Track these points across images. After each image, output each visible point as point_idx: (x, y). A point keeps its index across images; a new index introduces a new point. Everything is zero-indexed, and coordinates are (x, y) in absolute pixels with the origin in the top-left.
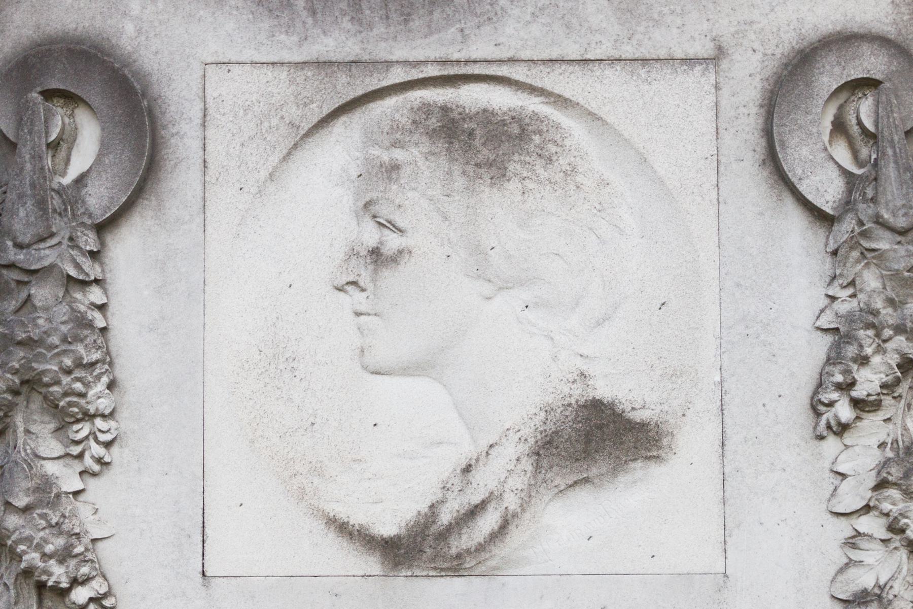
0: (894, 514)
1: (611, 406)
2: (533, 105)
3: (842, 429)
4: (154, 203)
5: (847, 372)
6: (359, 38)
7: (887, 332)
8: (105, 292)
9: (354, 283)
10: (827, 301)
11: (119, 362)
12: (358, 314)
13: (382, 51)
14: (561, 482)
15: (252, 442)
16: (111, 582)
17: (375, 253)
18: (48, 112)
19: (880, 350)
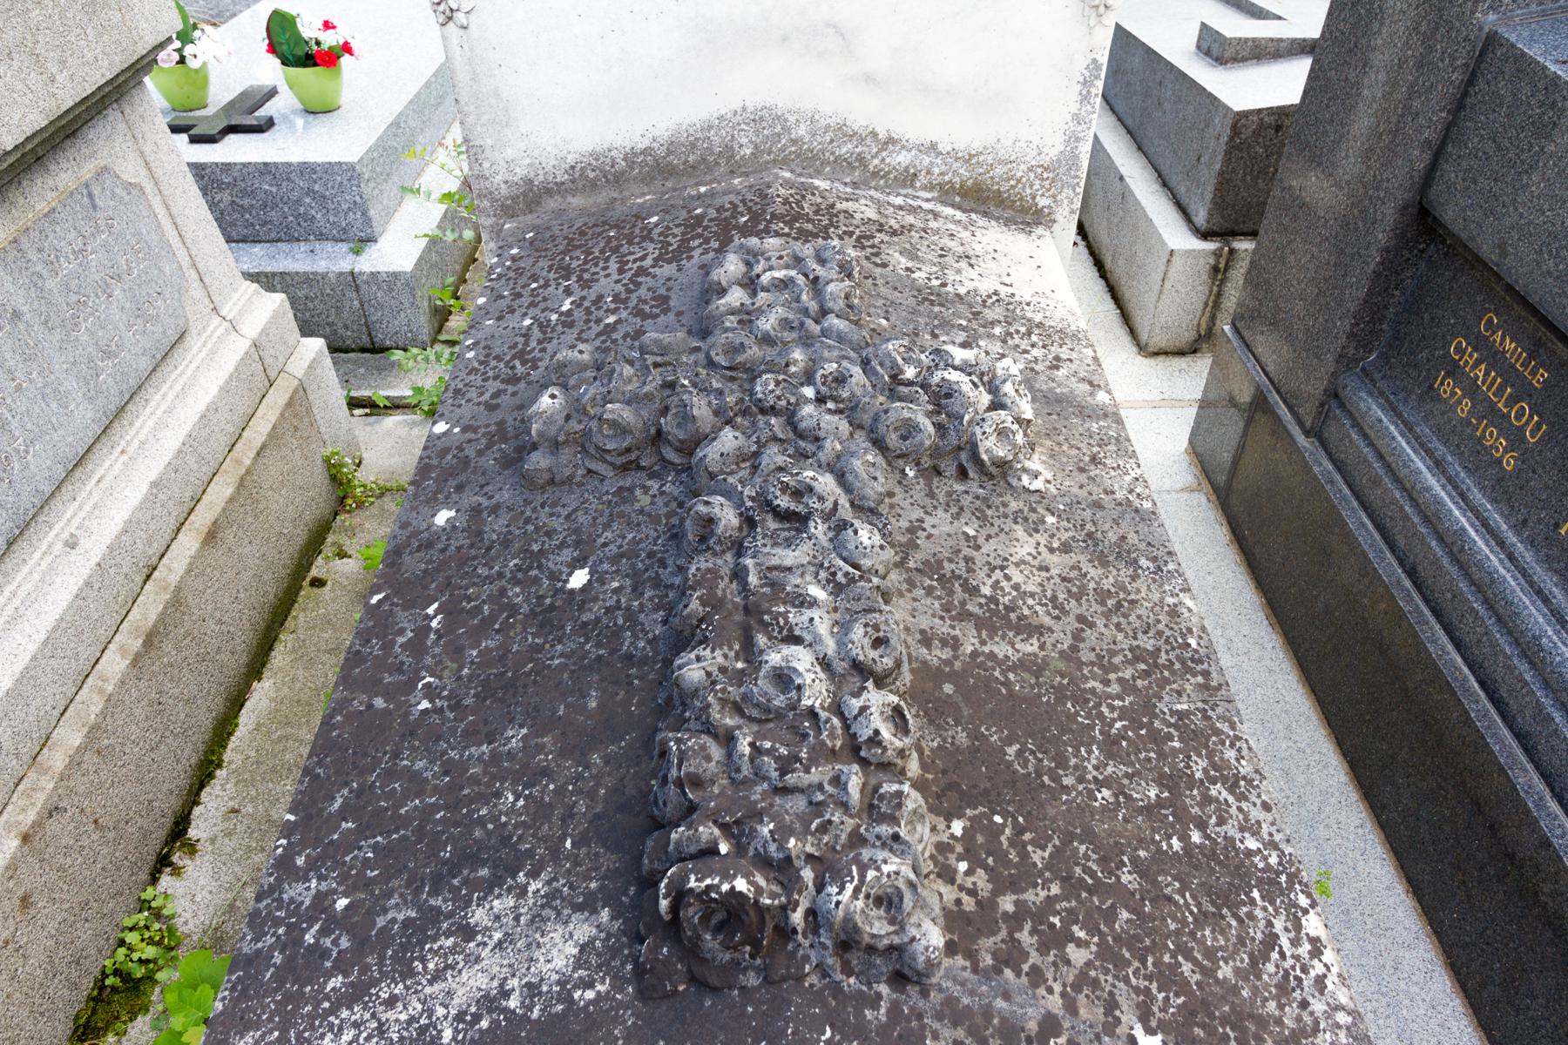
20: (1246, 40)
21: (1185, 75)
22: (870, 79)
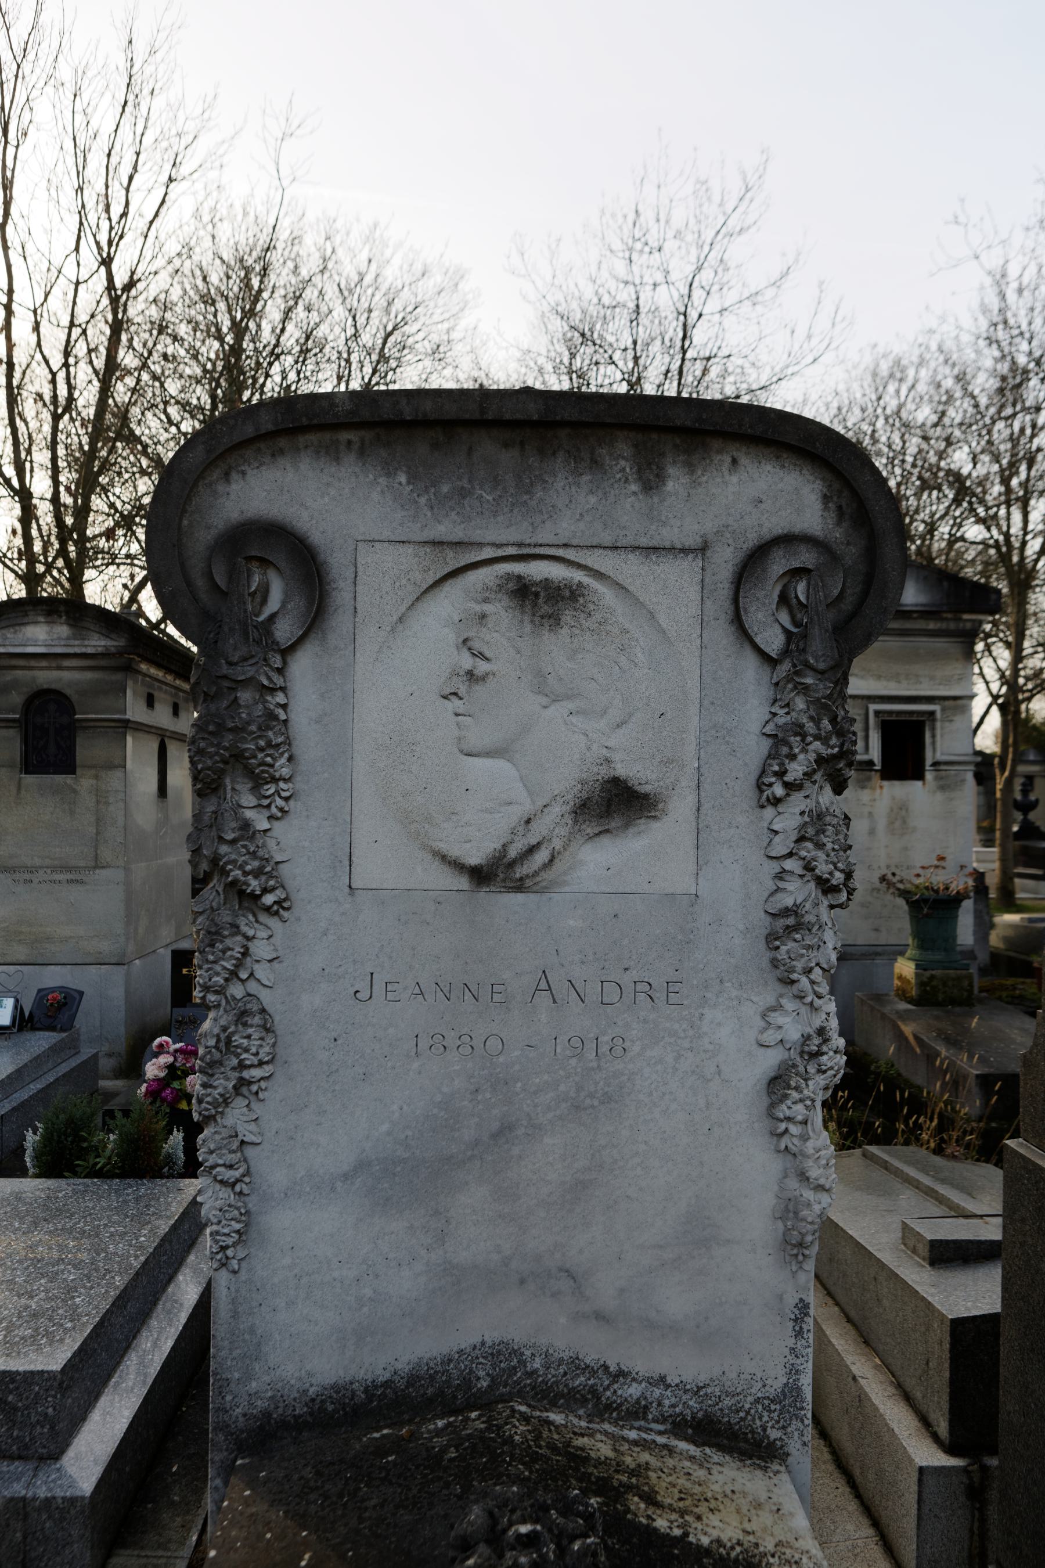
0: (808, 859)
1: (625, 782)
2: (578, 576)
3: (776, 802)
4: (320, 635)
5: (782, 764)
6: (463, 526)
7: (809, 739)
8: (286, 696)
9: (455, 694)
10: (770, 716)
11: (295, 743)
12: (457, 715)
13: (477, 535)
14: (589, 830)
15: (384, 799)
16: (289, 890)
17: (470, 674)
18: (249, 570)
19: (804, 750)
20: (947, 1242)
22: (600, 1316)
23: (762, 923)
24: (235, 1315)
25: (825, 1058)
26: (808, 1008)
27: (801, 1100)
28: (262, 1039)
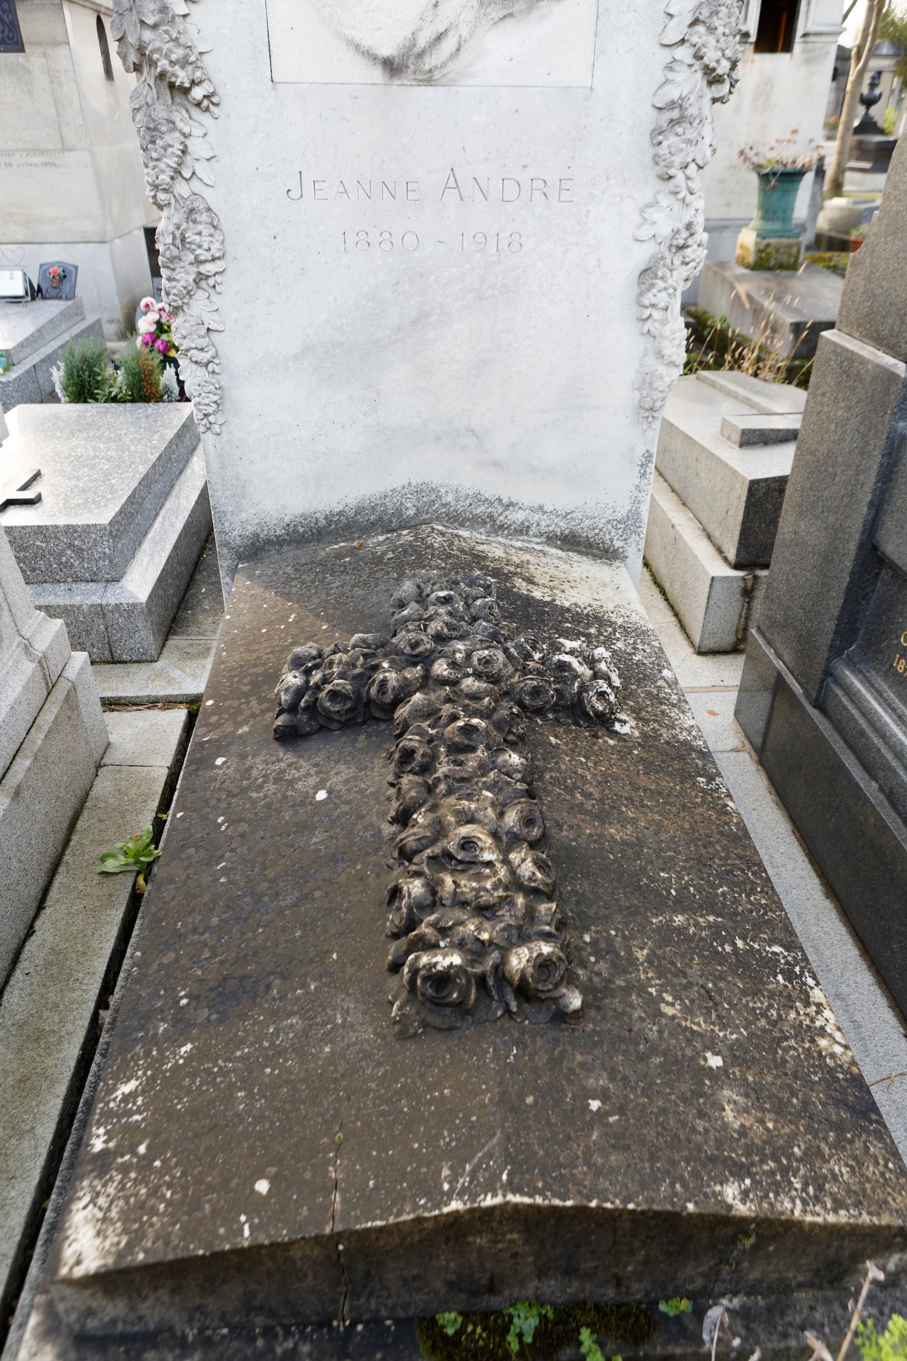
20: (755, 430)
21: (713, 455)
22: (496, 464)
23: (649, 119)
24: (223, 467)
25: (688, 251)
26: (680, 203)
27: (665, 289)
28: (211, 235)
